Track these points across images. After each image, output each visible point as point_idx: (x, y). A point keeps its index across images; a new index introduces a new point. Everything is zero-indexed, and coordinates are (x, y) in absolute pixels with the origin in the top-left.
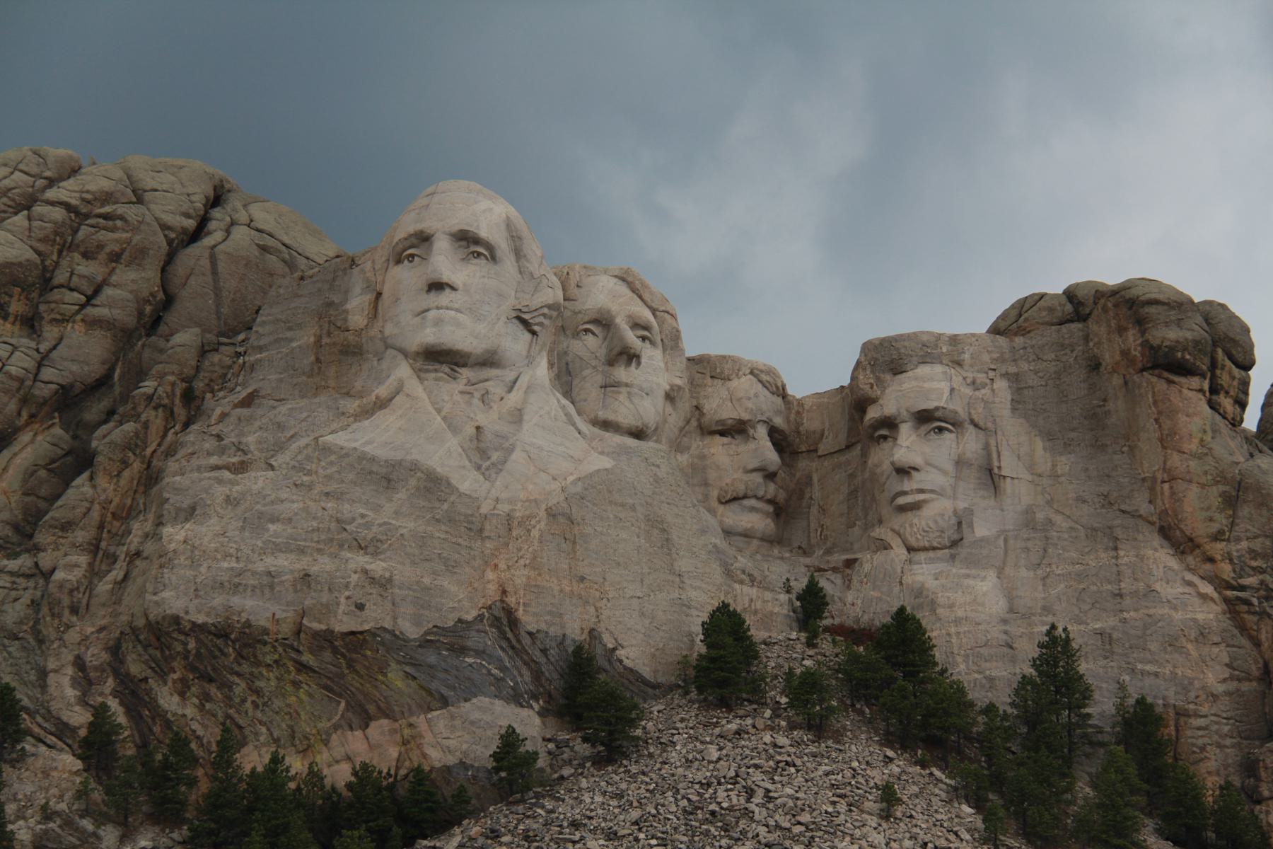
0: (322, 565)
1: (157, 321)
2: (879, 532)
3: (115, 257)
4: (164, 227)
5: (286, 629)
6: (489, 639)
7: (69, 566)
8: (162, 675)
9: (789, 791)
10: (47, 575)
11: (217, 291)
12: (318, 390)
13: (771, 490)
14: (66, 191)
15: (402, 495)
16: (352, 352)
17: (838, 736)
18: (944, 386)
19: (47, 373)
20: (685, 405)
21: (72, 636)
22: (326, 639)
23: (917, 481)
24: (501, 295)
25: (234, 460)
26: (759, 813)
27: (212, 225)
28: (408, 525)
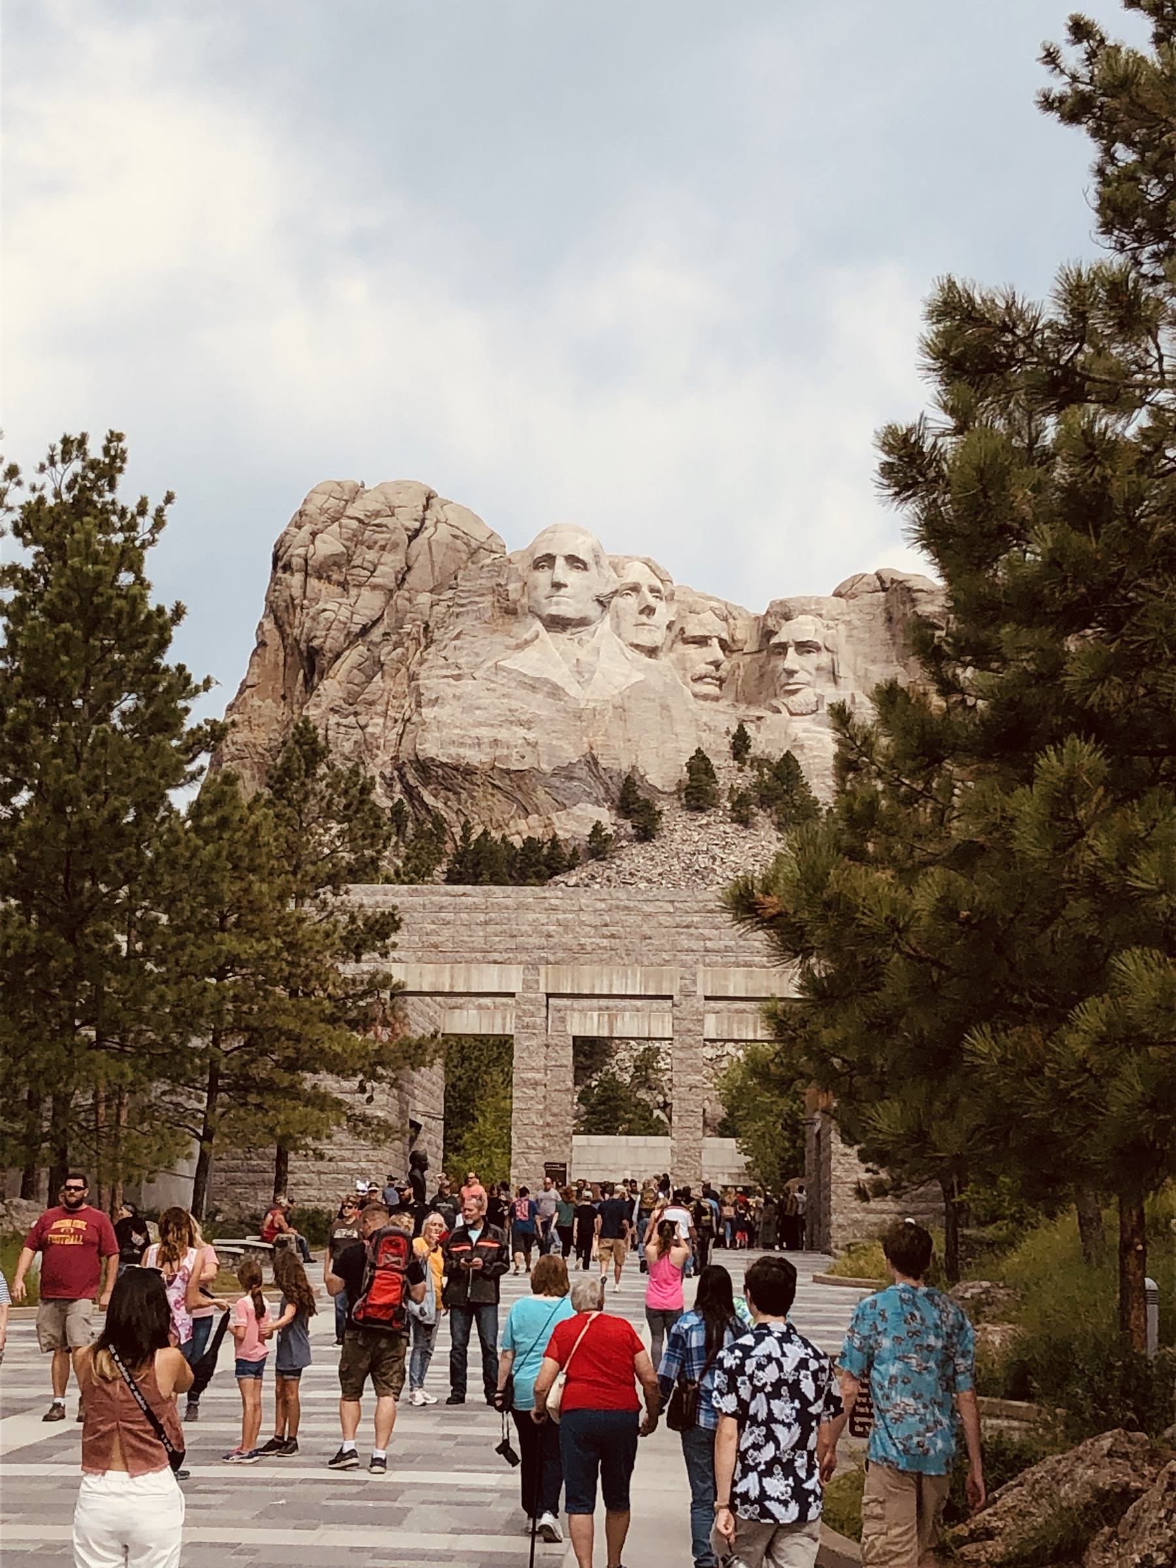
0: (503, 734)
1: (404, 579)
2: (775, 702)
3: (383, 548)
4: (407, 529)
5: (487, 767)
6: (582, 772)
7: (376, 726)
8: (425, 786)
9: (732, 858)
10: (363, 728)
11: (432, 562)
12: (495, 631)
13: (718, 675)
14: (355, 510)
15: (540, 696)
16: (511, 612)
17: (754, 826)
18: (812, 628)
19: (356, 618)
20: (676, 628)
21: (378, 761)
22: (508, 772)
23: (797, 678)
24: (589, 588)
25: (456, 672)
26: (719, 871)
27: (427, 523)
28: (543, 713)
